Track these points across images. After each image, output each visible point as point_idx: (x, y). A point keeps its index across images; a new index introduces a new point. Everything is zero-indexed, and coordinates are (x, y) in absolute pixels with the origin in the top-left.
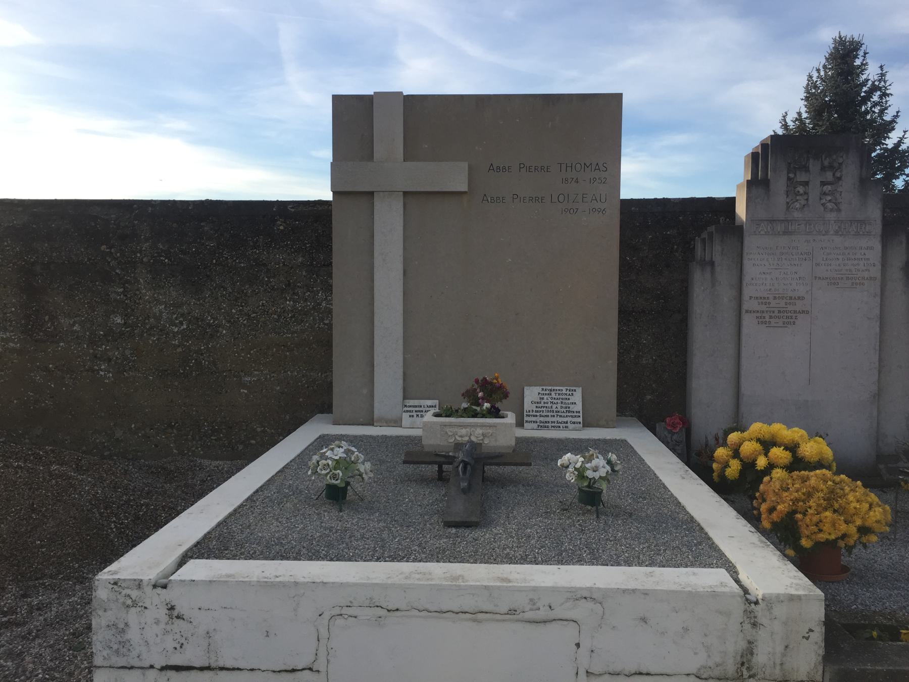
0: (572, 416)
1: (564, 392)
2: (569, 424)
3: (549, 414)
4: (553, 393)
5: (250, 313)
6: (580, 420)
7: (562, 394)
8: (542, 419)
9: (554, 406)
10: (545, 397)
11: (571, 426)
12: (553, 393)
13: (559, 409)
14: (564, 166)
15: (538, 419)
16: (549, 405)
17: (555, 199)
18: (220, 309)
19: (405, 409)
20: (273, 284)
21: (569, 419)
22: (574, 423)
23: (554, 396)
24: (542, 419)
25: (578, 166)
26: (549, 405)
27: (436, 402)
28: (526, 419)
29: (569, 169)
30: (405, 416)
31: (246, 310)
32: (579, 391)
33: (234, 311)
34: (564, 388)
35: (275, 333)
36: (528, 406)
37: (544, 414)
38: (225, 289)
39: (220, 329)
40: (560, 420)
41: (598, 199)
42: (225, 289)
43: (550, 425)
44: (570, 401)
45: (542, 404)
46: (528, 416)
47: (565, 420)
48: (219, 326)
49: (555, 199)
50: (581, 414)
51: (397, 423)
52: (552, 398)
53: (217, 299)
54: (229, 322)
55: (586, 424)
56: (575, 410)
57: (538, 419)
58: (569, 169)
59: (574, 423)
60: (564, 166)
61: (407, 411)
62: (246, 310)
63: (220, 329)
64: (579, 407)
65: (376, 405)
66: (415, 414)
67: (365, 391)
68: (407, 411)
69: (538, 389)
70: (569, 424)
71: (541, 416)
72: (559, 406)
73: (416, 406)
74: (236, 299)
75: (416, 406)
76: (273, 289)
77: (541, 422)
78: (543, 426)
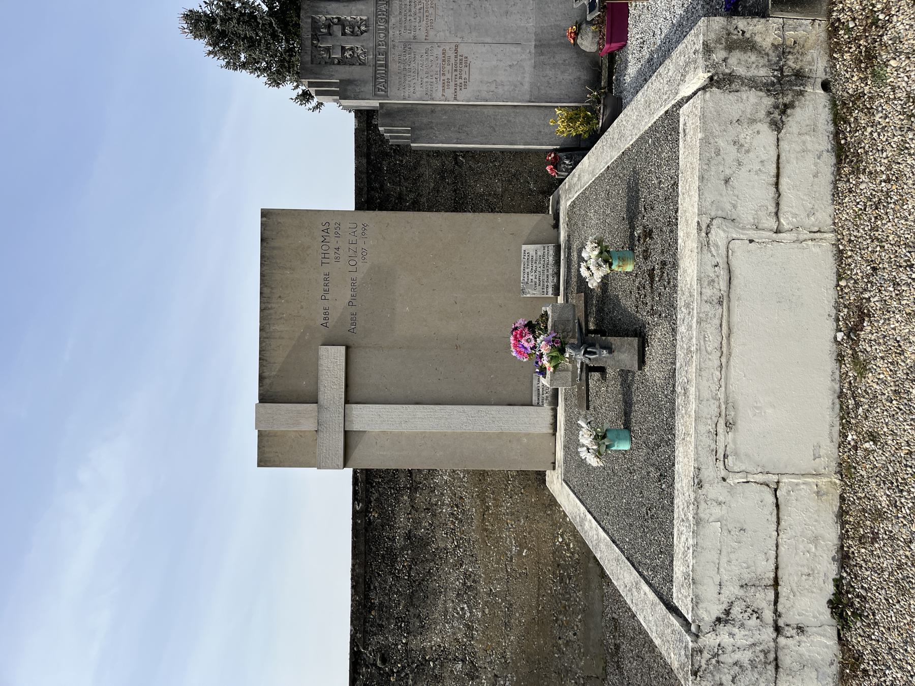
10: (530, 277)
14: (324, 261)
17: (354, 269)
29: (327, 256)
32: (524, 247)
45: (537, 280)
49: (354, 269)
58: (327, 256)
60: (324, 261)
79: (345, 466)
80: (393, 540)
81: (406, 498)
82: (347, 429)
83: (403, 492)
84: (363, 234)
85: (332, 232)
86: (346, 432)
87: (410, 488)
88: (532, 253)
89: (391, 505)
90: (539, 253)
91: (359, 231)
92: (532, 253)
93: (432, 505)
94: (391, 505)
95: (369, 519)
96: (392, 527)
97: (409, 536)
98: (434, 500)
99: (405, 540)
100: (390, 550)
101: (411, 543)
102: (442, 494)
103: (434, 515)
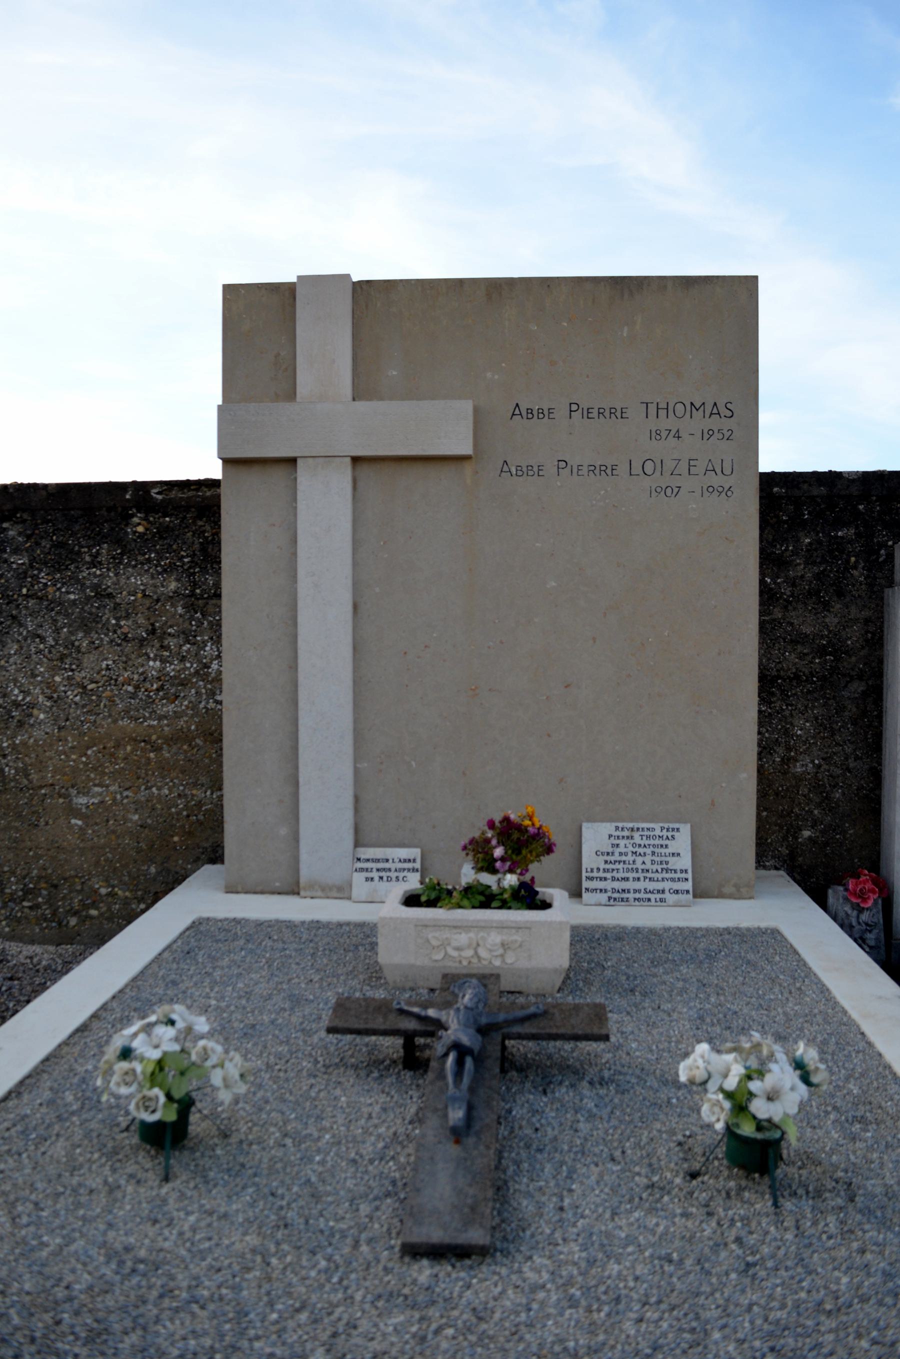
0: (673, 880)
1: (658, 832)
2: (667, 895)
3: (631, 875)
4: (636, 835)
5: (86, 682)
6: (689, 886)
8: (617, 885)
9: (639, 860)
10: (622, 843)
11: (671, 898)
12: (636, 835)
13: (648, 866)
15: (609, 885)
16: (630, 858)
18: (34, 676)
19: (359, 865)
20: (125, 630)
21: (667, 885)
23: (637, 840)
24: (617, 885)
26: (630, 858)
27: (415, 853)
28: (585, 884)
30: (359, 878)
31: (78, 676)
33: (57, 679)
34: (657, 826)
35: (130, 718)
36: (589, 860)
37: (620, 875)
38: (43, 639)
39: (35, 712)
40: (651, 886)
42: (43, 639)
43: (631, 896)
44: (667, 851)
45: (617, 857)
47: (660, 886)
48: (32, 705)
50: (689, 876)
51: (342, 891)
53: (28, 657)
54: (50, 698)
55: (699, 893)
56: (678, 867)
57: (609, 885)
61: (362, 870)
62: (78, 676)
63: (35, 712)
64: (685, 861)
65: (304, 856)
66: (375, 875)
67: (283, 831)
68: (362, 870)
69: (608, 828)
70: (667, 895)
71: (613, 879)
72: (648, 859)
73: (378, 861)
74: (62, 658)
75: (378, 861)
76: (125, 639)
77: (614, 890)
78: (618, 898)
79: (228, 462)
80: (94, 564)
81: (173, 585)
82: (299, 461)
83: (185, 579)
86: (292, 461)
87: (193, 594)
88: (673, 847)
89: (160, 557)
90: (671, 860)
92: (673, 847)
93: (161, 639)
94: (160, 557)
95: (133, 516)
96: (116, 561)
97: (101, 594)
98: (172, 642)
99: (96, 587)
100: (74, 556)
101: (88, 598)
102: (183, 659)
103: (142, 641)
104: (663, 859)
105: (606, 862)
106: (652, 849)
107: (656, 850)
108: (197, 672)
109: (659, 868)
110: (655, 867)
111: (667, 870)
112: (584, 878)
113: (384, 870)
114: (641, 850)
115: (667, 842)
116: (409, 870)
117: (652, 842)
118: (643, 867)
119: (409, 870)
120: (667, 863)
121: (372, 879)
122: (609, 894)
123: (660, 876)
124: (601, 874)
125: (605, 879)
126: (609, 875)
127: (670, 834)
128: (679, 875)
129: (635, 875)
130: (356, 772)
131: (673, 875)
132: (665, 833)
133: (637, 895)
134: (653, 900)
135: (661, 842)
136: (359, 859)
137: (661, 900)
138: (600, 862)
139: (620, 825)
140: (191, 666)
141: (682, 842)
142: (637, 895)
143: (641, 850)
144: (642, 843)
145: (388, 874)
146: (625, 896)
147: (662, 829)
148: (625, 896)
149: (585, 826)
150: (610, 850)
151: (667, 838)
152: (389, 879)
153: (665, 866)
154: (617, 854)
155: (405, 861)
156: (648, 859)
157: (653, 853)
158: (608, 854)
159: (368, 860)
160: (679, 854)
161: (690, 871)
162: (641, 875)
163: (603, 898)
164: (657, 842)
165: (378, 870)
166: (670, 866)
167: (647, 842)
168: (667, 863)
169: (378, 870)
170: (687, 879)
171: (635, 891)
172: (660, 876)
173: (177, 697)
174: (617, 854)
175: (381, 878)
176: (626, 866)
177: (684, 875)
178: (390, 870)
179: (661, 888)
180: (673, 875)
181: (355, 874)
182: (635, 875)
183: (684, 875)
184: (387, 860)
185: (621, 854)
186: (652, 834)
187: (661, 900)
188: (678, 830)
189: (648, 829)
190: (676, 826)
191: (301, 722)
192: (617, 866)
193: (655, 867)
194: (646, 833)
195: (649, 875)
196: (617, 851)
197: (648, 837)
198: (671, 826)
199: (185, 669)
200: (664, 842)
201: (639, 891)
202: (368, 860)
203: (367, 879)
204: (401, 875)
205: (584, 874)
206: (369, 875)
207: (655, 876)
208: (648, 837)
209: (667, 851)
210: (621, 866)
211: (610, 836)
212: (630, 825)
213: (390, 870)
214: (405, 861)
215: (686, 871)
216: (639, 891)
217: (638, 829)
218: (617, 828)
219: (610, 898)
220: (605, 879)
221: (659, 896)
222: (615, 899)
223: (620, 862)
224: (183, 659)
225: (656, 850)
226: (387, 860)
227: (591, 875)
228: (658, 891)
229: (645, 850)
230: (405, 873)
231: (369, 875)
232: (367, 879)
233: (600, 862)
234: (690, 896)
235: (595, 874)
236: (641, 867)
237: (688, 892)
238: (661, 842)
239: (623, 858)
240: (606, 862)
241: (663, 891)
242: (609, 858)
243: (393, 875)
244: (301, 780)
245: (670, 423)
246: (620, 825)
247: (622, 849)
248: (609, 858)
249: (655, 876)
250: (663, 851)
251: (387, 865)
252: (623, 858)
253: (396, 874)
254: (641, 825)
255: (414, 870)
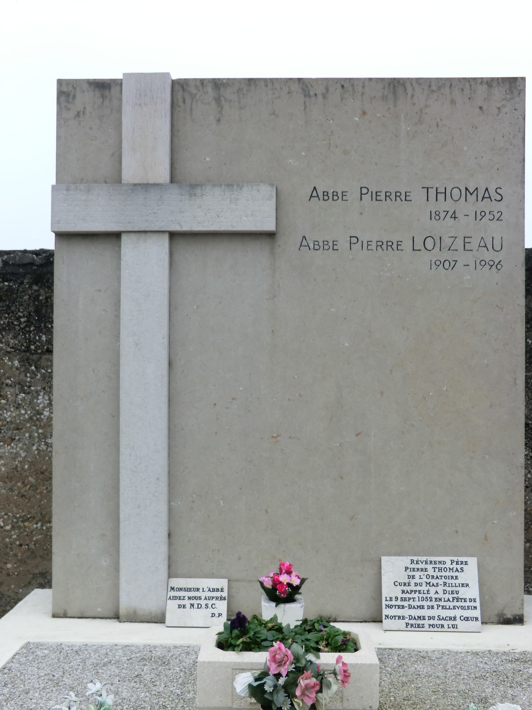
0: (463, 608)
1: (448, 565)
2: (458, 622)
3: (425, 604)
6: (477, 613)
7: (445, 570)
9: (433, 590)
10: (417, 574)
13: (441, 595)
14: (432, 192)
15: (406, 612)
16: (424, 588)
17: (419, 245)
19: (172, 594)
21: (458, 613)
22: (467, 619)
23: (431, 572)
25: (456, 192)
26: (424, 588)
28: (386, 612)
29: (441, 197)
30: (172, 605)
32: (473, 562)
34: (448, 559)
36: (388, 590)
41: (490, 247)
43: (426, 622)
44: (457, 582)
45: (413, 588)
46: (388, 606)
49: (419, 245)
50: (478, 604)
52: (428, 577)
56: (468, 597)
57: (406, 612)
58: (441, 197)
59: (467, 619)
60: (432, 192)
61: (175, 598)
64: (473, 592)
66: (187, 603)
68: (175, 598)
69: (405, 561)
70: (458, 622)
71: (410, 607)
72: (440, 589)
73: (189, 590)
75: (189, 590)
77: (411, 617)
78: (415, 625)
84: (483, 263)
85: (486, 206)
88: (463, 578)
90: (461, 590)
91: (488, 256)
92: (463, 578)
104: (454, 589)
105: (403, 592)
106: (444, 580)
107: (448, 581)
108: (31, 418)
109: (450, 597)
110: (447, 596)
111: (458, 600)
112: (384, 606)
113: (195, 598)
114: (434, 581)
115: (457, 574)
116: (217, 598)
117: (443, 574)
118: (436, 596)
119: (217, 598)
120: (457, 593)
121: (184, 606)
122: (407, 620)
123: (451, 604)
124: (399, 603)
125: (403, 607)
126: (406, 604)
127: (459, 567)
128: (468, 604)
129: (429, 603)
130: (170, 510)
131: (463, 604)
132: (454, 566)
133: (432, 622)
134: (446, 626)
135: (451, 574)
136: (172, 589)
137: (454, 626)
138: (397, 592)
139: (415, 558)
140: (25, 413)
141: (470, 574)
142: (432, 622)
143: (434, 581)
144: (435, 574)
145: (198, 602)
146: (421, 622)
147: (452, 562)
148: (421, 622)
149: (384, 559)
150: (407, 581)
151: (457, 570)
152: (199, 606)
153: (455, 595)
154: (412, 584)
155: (214, 590)
156: (440, 589)
157: (445, 584)
158: (405, 584)
159: (180, 589)
160: (467, 585)
161: (478, 600)
162: (435, 604)
163: (402, 624)
164: (448, 574)
165: (189, 598)
166: (460, 596)
167: (439, 574)
168: (457, 593)
169: (189, 598)
170: (475, 608)
171: (430, 618)
172: (451, 604)
173: (13, 440)
174: (412, 584)
175: (192, 605)
176: (421, 596)
177: (472, 604)
178: (200, 598)
179: (453, 616)
180: (463, 604)
181: (169, 601)
182: (429, 603)
183: (472, 604)
184: (198, 590)
185: (416, 585)
186: (443, 566)
187: (454, 626)
188: (466, 563)
189: (440, 562)
190: (464, 559)
191: (122, 465)
192: (413, 595)
193: (447, 596)
194: (437, 566)
195: (442, 603)
196: (413, 582)
197: (440, 570)
198: (461, 559)
199: (20, 415)
200: (455, 574)
201: (433, 618)
202: (180, 589)
203: (179, 606)
204: (210, 603)
205: (384, 603)
206: (182, 602)
207: (447, 604)
208: (440, 570)
209: (457, 582)
210: (416, 595)
211: (406, 568)
212: (424, 558)
213: (200, 598)
214: (214, 590)
215: (475, 600)
216: (433, 618)
217: (431, 562)
218: (412, 561)
219: (407, 624)
220: (403, 607)
221: (451, 623)
222: (412, 625)
223: (415, 592)
224: (18, 407)
225: (448, 581)
226: (198, 590)
227: (390, 603)
228: (450, 619)
229: (437, 581)
230: (214, 601)
231: (182, 602)
232: (179, 606)
233: (397, 592)
234: (479, 623)
235: (394, 603)
236: (434, 596)
237: (477, 619)
238: (451, 574)
239: (418, 588)
240: (403, 592)
241: (455, 618)
242: (406, 588)
243: (203, 602)
244: (121, 516)
245: (448, 205)
246: (415, 558)
247: (417, 580)
248: (406, 588)
249: (447, 604)
250: (453, 581)
251: (197, 594)
252: (418, 588)
253: (206, 602)
254: (433, 559)
255: (222, 598)
